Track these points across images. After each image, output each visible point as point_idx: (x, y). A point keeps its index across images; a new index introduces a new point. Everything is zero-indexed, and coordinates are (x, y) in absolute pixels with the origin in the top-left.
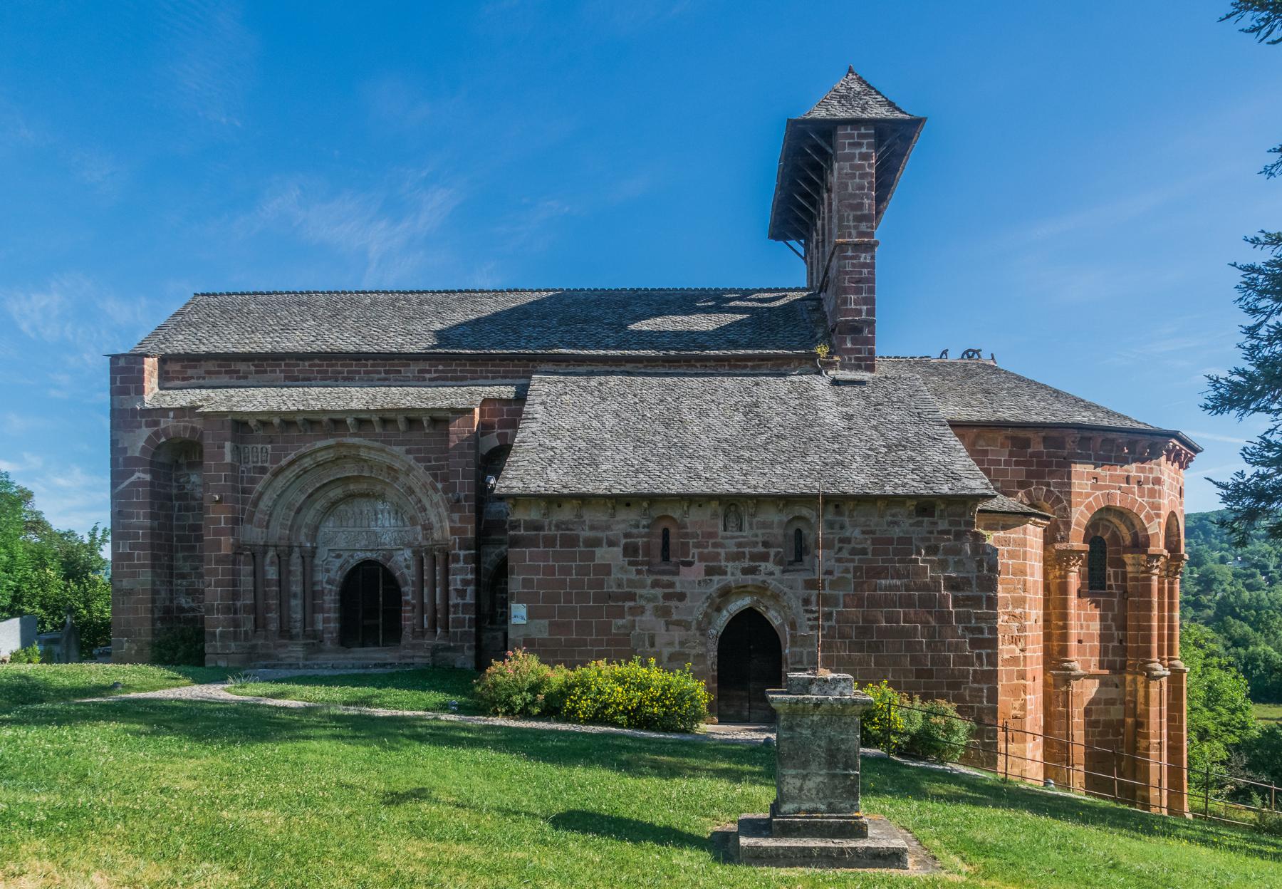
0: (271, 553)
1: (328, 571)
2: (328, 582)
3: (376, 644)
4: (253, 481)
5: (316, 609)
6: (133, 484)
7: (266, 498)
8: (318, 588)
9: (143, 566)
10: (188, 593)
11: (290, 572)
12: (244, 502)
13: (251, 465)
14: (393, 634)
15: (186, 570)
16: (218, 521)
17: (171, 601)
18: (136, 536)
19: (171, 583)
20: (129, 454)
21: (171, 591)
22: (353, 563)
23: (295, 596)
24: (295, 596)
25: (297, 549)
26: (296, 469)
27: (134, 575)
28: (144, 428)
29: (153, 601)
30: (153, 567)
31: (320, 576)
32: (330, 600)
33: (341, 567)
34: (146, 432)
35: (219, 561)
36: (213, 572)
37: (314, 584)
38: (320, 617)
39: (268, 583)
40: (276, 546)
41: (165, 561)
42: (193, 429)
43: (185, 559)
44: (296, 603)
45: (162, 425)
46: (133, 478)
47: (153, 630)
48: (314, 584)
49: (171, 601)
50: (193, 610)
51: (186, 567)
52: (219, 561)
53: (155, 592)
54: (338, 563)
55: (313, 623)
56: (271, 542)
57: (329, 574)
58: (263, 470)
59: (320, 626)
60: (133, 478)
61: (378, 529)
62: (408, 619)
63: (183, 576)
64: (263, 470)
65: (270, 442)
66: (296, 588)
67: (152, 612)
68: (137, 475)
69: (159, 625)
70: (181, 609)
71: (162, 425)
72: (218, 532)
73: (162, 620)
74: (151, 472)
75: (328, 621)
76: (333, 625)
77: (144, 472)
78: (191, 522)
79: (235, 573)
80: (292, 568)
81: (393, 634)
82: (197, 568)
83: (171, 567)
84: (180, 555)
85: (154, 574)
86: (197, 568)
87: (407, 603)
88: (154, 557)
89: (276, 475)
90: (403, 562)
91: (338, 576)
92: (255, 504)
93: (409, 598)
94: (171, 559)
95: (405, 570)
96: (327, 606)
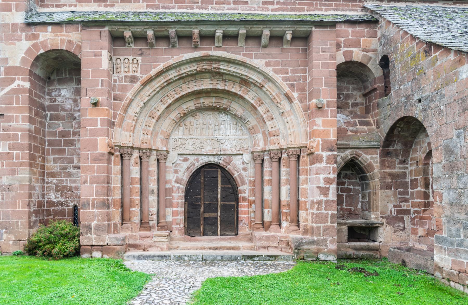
0: (136, 154)
2: (177, 182)
3: (215, 233)
4: (124, 89)
6: (15, 91)
7: (134, 104)
8: (168, 186)
9: (22, 164)
10: (57, 189)
11: (149, 172)
12: (115, 108)
13: (123, 74)
14: (231, 225)
15: (56, 170)
16: (94, 122)
17: (43, 196)
18: (15, 137)
19: (43, 180)
20: (11, 63)
21: (43, 187)
22: (198, 165)
25: (154, 153)
26: (162, 80)
27: (13, 172)
28: (24, 41)
29: (30, 196)
30: (30, 165)
31: (171, 176)
32: (178, 197)
33: (188, 168)
34: (25, 45)
35: (96, 159)
36: (91, 169)
37: (166, 182)
38: (169, 211)
40: (139, 149)
41: (39, 161)
42: (70, 42)
43: (55, 160)
44: (153, 199)
45: (41, 39)
46: (13, 86)
47: (30, 222)
48: (166, 182)
49: (43, 196)
50: (61, 204)
52: (96, 159)
53: (32, 188)
56: (137, 145)
57: (178, 175)
58: (133, 79)
59: (170, 218)
60: (13, 86)
61: (220, 137)
62: (246, 213)
63: (53, 175)
64: (133, 79)
66: (153, 186)
67: (29, 205)
69: (34, 218)
70: (51, 203)
71: (41, 39)
72: (94, 133)
73: (36, 212)
74: (30, 80)
75: (176, 214)
76: (181, 218)
77: (23, 80)
78: (61, 129)
79: (109, 171)
80: (151, 169)
81: (231, 225)
83: (43, 167)
84: (51, 157)
85: (32, 172)
87: (244, 199)
88: (32, 158)
89: (145, 84)
90: (242, 169)
91: (185, 177)
92: (126, 111)
93: (246, 195)
94: (44, 160)
95: (243, 172)
96: (175, 201)
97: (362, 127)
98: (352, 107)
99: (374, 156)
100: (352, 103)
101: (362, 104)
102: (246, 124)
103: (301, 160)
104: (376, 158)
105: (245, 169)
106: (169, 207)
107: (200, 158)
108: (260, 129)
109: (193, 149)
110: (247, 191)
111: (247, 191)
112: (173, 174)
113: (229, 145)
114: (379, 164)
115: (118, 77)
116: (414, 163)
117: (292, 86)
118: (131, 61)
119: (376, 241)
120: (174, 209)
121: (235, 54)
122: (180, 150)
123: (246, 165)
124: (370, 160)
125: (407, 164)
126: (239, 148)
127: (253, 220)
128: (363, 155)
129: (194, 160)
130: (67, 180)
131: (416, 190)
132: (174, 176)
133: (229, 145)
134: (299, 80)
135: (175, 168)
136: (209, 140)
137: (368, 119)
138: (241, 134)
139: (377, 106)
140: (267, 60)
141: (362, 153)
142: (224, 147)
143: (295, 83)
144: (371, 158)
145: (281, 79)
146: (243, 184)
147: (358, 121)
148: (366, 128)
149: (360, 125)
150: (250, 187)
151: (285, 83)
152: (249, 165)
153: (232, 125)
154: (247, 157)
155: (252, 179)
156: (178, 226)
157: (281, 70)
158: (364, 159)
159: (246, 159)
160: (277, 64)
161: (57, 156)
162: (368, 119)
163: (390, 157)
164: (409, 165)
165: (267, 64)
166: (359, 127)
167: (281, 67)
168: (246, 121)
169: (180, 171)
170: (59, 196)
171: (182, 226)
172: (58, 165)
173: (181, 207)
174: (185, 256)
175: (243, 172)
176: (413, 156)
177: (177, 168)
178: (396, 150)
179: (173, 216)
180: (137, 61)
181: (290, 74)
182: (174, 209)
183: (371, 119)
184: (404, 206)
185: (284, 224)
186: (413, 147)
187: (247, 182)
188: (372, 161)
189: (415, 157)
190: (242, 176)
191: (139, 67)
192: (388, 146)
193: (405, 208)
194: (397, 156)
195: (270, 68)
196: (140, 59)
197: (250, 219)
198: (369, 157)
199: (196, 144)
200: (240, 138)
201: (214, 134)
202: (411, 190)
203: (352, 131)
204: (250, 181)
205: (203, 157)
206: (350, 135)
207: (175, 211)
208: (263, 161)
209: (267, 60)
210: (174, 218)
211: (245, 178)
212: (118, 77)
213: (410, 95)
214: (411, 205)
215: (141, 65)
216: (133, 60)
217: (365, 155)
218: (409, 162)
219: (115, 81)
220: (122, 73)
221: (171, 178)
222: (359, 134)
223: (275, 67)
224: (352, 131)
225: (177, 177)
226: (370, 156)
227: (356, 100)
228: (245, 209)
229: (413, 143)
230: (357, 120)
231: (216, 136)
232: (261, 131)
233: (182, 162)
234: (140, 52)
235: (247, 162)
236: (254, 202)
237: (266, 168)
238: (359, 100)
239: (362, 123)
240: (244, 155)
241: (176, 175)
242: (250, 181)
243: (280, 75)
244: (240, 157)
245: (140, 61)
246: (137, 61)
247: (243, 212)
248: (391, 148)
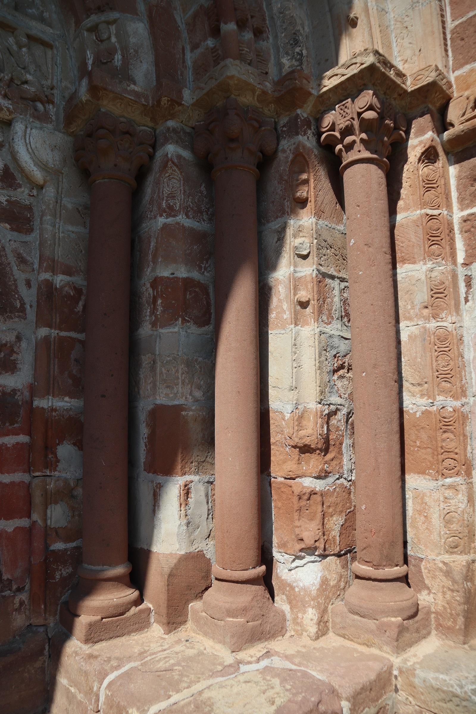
110: (26, 357)
111: (26, 357)
123: (23, 195)
127: (58, 546)
150: (43, 332)
152: (50, 192)
155: (60, 280)
159: (32, 154)
187: (29, 296)
197: (38, 544)
204: (48, 292)
211: (19, 275)
235: (38, 175)
236: (74, 429)
240: (19, 127)
242: (48, 292)
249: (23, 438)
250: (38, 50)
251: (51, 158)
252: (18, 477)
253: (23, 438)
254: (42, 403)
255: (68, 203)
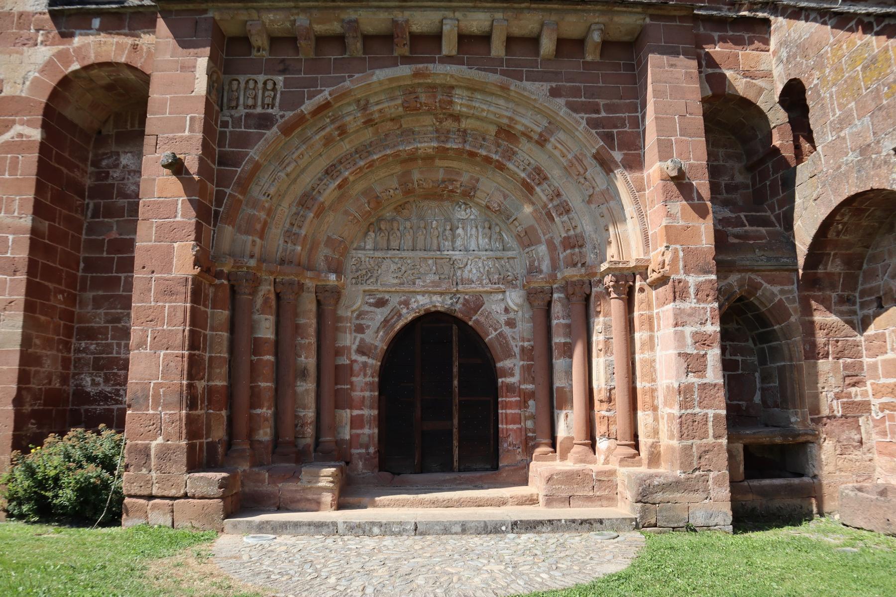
1: (360, 329)
2: (361, 351)
5: (342, 400)
8: (344, 361)
10: (98, 365)
15: (99, 322)
19: (67, 346)
21: (66, 362)
23: (303, 374)
24: (303, 374)
31: (349, 340)
32: (363, 384)
37: (338, 352)
38: (346, 415)
39: (257, 346)
41: (58, 301)
43: (97, 302)
44: (307, 388)
48: (338, 352)
49: (64, 380)
50: (104, 397)
51: (99, 319)
54: (380, 314)
55: (335, 428)
57: (364, 337)
61: (457, 255)
63: (90, 334)
65: (282, 72)
66: (308, 360)
68: (18, 129)
75: (359, 422)
76: (370, 432)
80: (302, 321)
82: (117, 319)
84: (90, 295)
86: (117, 319)
91: (379, 340)
94: (72, 300)
95: (507, 330)
96: (357, 394)
97: (755, 228)
98: (727, 192)
99: (786, 288)
100: (726, 184)
101: (746, 187)
102: (511, 226)
103: (638, 296)
104: (790, 292)
105: (511, 323)
106: (344, 408)
107: (413, 300)
108: (542, 235)
109: (396, 281)
111: (517, 371)
112: (354, 334)
113: (474, 271)
114: (797, 305)
115: (231, 116)
116: (871, 301)
117: (608, 138)
118: (260, 85)
119: (801, 475)
120: (356, 412)
121: (485, 70)
122: (368, 282)
123: (512, 315)
124: (779, 297)
125: (854, 304)
126: (496, 277)
127: (530, 434)
128: (765, 284)
129: (400, 303)
130: (119, 345)
131: (880, 358)
132: (355, 339)
133: (474, 271)
134: (624, 126)
135: (358, 322)
136: (430, 262)
137: (763, 214)
138: (501, 248)
139: (782, 185)
140: (554, 85)
141: (763, 282)
142: (466, 274)
143: (615, 131)
144: (782, 292)
145: (584, 122)
146: (509, 354)
147: (745, 216)
148: (763, 230)
149: (751, 225)
150: (522, 363)
151: (594, 131)
152: (520, 313)
153: (480, 230)
154: (514, 298)
155: (526, 344)
156: (364, 451)
157: (583, 103)
158: (768, 294)
159: (512, 301)
160: (576, 92)
161: (101, 293)
162: (763, 214)
163: (820, 290)
164: (857, 307)
165: (555, 93)
166: (748, 228)
167: (583, 99)
168: (511, 220)
169: (368, 327)
170: (100, 380)
171: (372, 450)
172: (101, 311)
173: (371, 408)
174: (373, 524)
175: (507, 330)
176: (868, 286)
177: (362, 322)
178: (830, 275)
179: (351, 428)
180: (275, 84)
181: (603, 114)
182: (356, 412)
183: (769, 213)
184: (856, 395)
185: (602, 444)
186: (865, 266)
187: (517, 350)
188: (783, 298)
189: (871, 289)
190: (505, 338)
191: (278, 96)
192: (816, 267)
193: (859, 399)
194: (833, 287)
195: (561, 101)
196: (280, 79)
197: (523, 433)
198: (776, 289)
199: (403, 269)
200: (499, 254)
201: (442, 248)
202: (868, 360)
203: (736, 236)
204: (523, 349)
205: (419, 297)
206: (734, 244)
207: (358, 416)
208: (549, 303)
209: (554, 85)
210: (354, 431)
211: (513, 343)
212: (231, 116)
213: (869, 145)
214: (870, 392)
215: (282, 93)
216: (265, 83)
217: (768, 286)
218: (858, 300)
219: (225, 124)
220: (241, 108)
221: (348, 343)
222: (751, 242)
223: (571, 99)
224: (736, 236)
225: (362, 340)
226: (779, 288)
227: (732, 179)
228: (513, 411)
229: (863, 259)
230: (742, 215)
231: (446, 253)
232: (543, 239)
233: (372, 309)
234: (281, 67)
235: (516, 308)
236: (532, 395)
237: (558, 318)
238: (739, 179)
239: (753, 221)
240: (508, 293)
241: (360, 336)
242: (523, 349)
243: (582, 115)
244: (500, 296)
245: (280, 85)
246: (275, 84)
247: (509, 418)
248: (821, 270)
249: (518, 399)
250: (511, 261)
251: (519, 301)
252: (517, 411)
253: (518, 399)
254: (522, 387)
255: (527, 316)
